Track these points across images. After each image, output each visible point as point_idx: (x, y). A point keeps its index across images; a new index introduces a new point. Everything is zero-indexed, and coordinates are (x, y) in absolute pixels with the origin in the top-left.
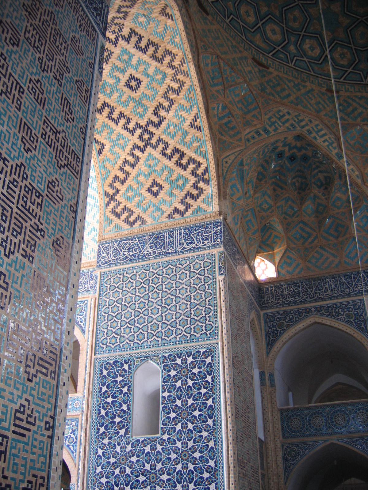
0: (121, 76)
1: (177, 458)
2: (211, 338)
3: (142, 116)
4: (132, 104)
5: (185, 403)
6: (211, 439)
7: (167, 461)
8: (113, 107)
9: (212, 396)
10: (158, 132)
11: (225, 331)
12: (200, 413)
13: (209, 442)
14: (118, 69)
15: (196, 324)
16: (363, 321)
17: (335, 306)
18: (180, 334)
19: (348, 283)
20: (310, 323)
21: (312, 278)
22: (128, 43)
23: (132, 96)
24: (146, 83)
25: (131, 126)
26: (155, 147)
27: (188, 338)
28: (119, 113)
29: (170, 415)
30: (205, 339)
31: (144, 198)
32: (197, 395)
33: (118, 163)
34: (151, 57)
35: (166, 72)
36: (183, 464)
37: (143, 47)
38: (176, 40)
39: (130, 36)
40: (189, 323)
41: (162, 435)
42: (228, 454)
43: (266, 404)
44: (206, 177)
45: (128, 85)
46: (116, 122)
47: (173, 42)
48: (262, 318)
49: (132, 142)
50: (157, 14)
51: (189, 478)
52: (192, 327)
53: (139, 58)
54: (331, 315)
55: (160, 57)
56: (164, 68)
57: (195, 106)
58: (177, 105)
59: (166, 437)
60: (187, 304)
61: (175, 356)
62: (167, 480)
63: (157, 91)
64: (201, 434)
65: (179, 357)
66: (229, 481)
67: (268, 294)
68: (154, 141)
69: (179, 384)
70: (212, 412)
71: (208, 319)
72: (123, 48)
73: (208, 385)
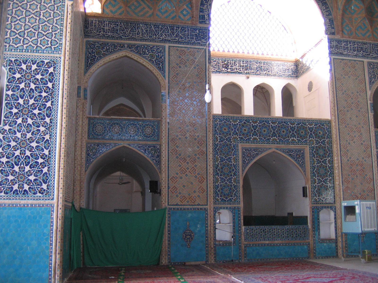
1: (16, 146)
2: (55, 52)
5: (26, 102)
6: (47, 133)
7: (6, 147)
9: (51, 99)
11: (68, 48)
12: (39, 112)
13: (45, 135)
15: (43, 38)
16: (161, 62)
17: (143, 47)
18: (27, 44)
19: (156, 31)
20: (122, 56)
21: (129, 21)
27: (35, 49)
29: (12, 111)
30: (50, 52)
32: (38, 97)
36: (21, 151)
40: (36, 36)
41: (4, 126)
42: (61, 146)
43: (79, 111)
48: (84, 44)
51: (25, 162)
52: (39, 40)
54: (139, 53)
59: (7, 128)
60: (36, 19)
61: (20, 62)
62: (6, 162)
64: (39, 128)
65: (25, 63)
66: (59, 167)
67: (92, 26)
69: (22, 86)
70: (50, 112)
71: (54, 35)
73: (48, 90)
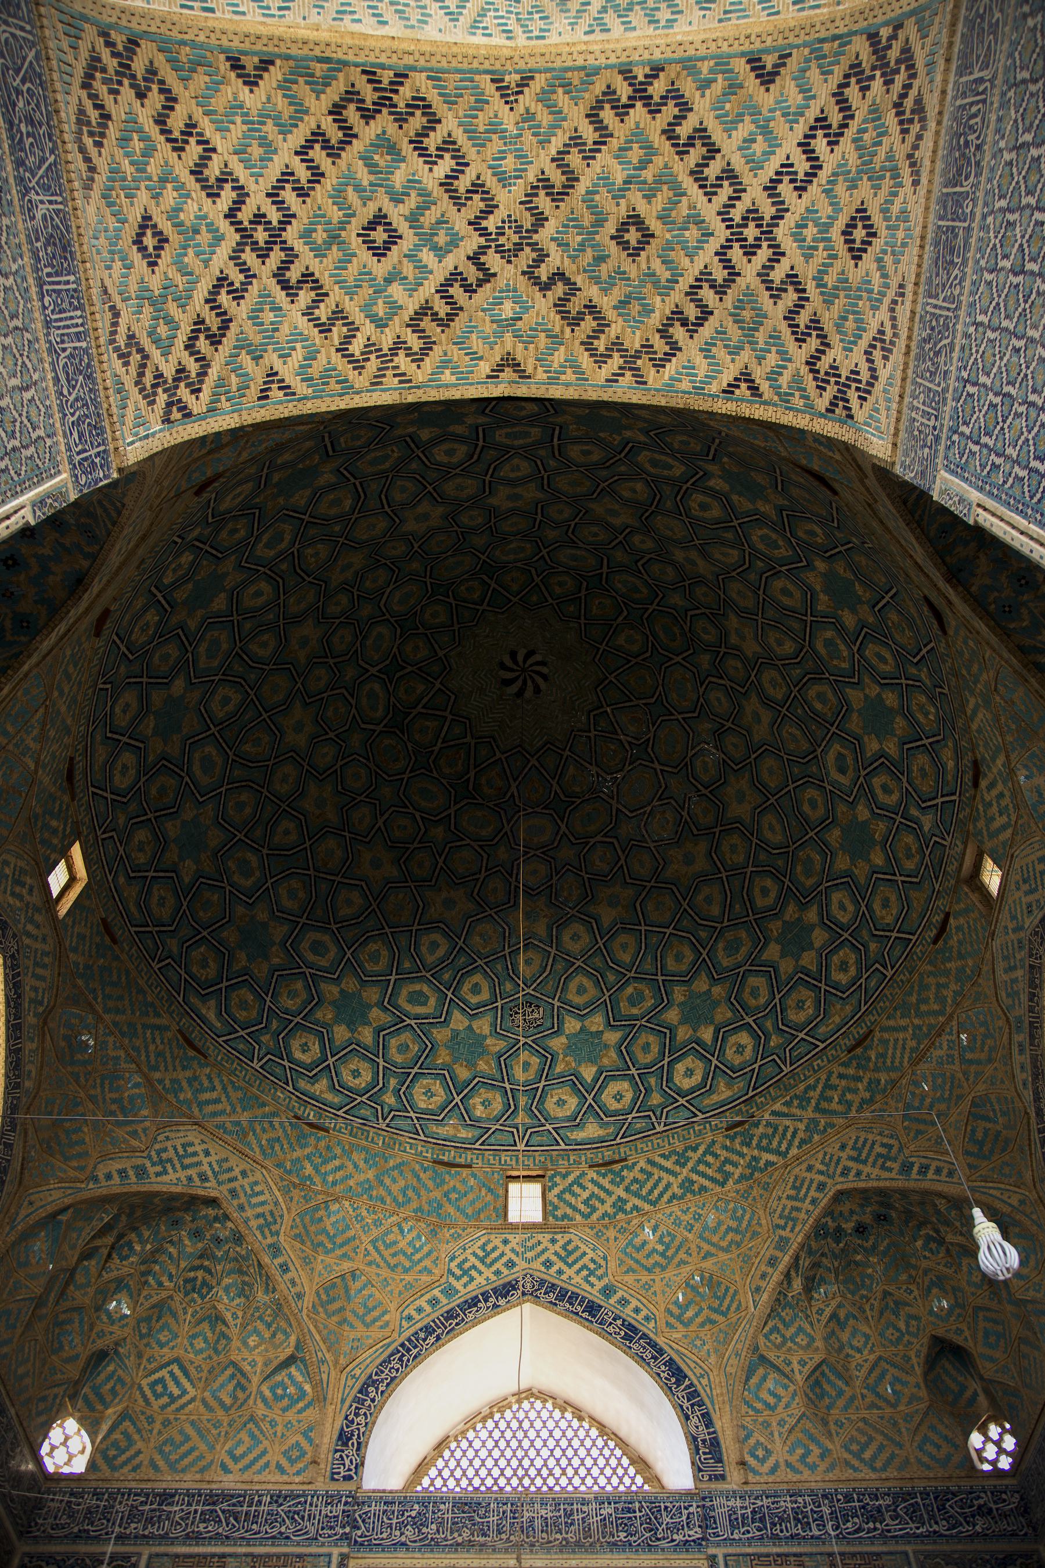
0: (404, 209)
4: (336, 214)
8: (339, 156)
10: (265, 271)
22: (469, 258)
33: (206, 119)
38: (447, 372)
39: (481, 267)
45: (379, 220)
49: (251, 187)
50: (509, 347)
56: (396, 327)
63: (351, 294)
68: (249, 257)
72: (462, 239)
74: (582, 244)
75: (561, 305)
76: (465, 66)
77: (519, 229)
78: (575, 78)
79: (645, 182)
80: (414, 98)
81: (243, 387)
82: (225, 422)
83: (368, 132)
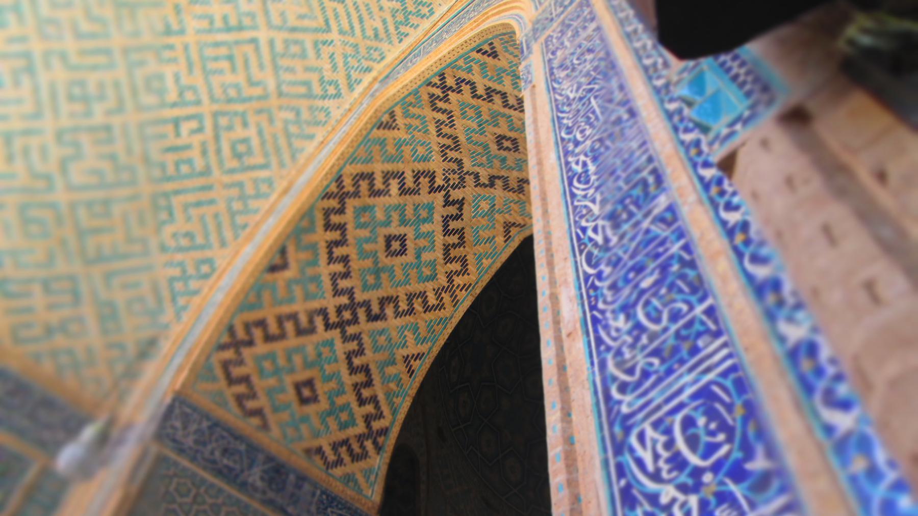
0: (395, 223)
3: (365, 287)
4: (368, 263)
10: (364, 326)
14: (402, 214)
22: (444, 206)
23: (379, 254)
24: (408, 261)
25: (343, 284)
26: (345, 339)
28: (345, 254)
31: (283, 390)
34: (444, 245)
35: (438, 276)
37: (450, 228)
38: (484, 261)
39: (453, 203)
44: (380, 440)
45: (389, 240)
46: (331, 259)
47: (479, 259)
50: (502, 221)
53: (433, 232)
55: (452, 256)
57: (429, 343)
58: (412, 321)
63: (407, 282)
72: (433, 203)
74: (488, 159)
75: (506, 187)
76: (360, 139)
77: (454, 172)
78: (411, 99)
79: (487, 121)
80: (353, 179)
81: (399, 383)
82: (404, 405)
83: (349, 216)
